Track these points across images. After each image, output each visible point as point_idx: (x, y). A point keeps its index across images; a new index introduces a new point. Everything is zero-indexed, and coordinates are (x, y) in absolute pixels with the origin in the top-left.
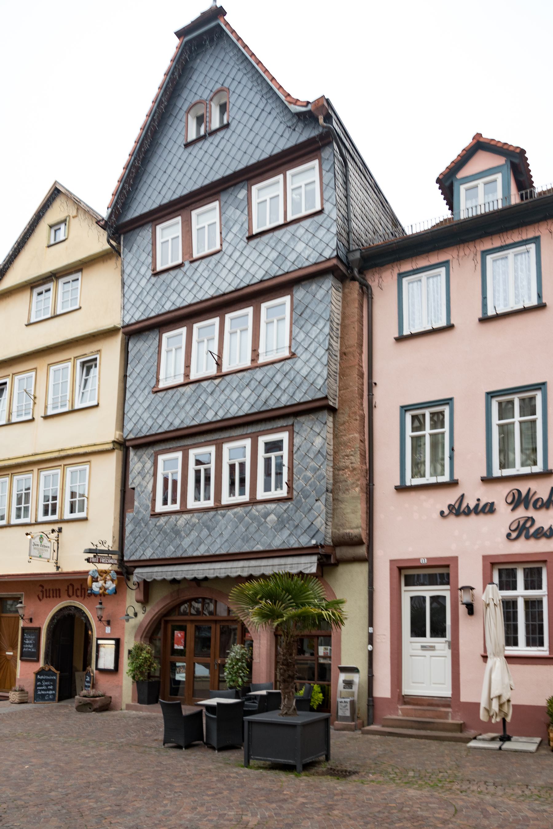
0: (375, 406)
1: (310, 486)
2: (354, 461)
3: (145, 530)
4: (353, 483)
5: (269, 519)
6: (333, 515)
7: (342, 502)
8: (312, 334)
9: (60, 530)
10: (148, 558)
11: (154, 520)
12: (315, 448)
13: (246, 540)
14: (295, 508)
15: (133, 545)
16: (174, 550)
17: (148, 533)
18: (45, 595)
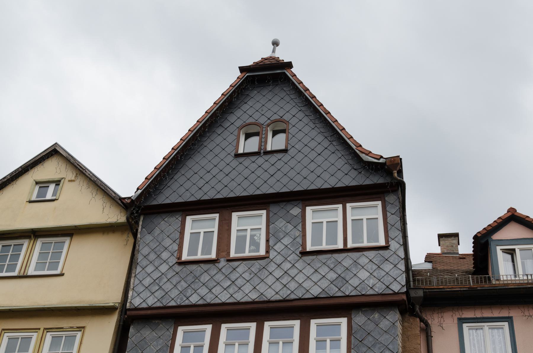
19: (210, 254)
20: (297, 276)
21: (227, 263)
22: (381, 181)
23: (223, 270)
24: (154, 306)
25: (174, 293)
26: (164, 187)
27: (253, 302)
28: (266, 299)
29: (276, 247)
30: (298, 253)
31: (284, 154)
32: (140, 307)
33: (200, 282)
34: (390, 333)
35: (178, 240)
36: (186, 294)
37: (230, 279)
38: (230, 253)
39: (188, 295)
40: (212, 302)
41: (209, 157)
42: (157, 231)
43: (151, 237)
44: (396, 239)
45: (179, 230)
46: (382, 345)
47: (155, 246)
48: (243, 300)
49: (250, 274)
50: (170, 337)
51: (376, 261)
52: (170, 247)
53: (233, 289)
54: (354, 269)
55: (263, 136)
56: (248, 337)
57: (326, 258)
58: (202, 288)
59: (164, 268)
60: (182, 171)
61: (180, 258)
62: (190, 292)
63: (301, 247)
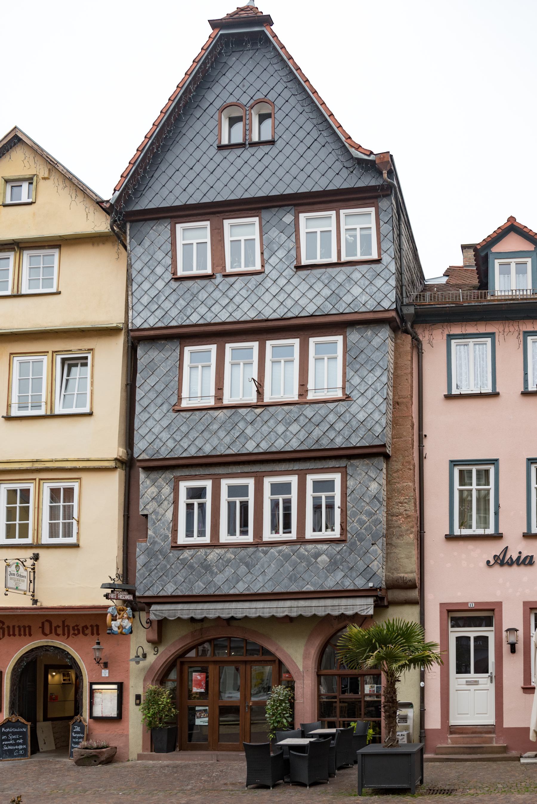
0: (425, 458)
1: (365, 529)
2: (408, 508)
3: (164, 562)
4: (408, 530)
5: (319, 559)
6: (387, 559)
7: (396, 547)
8: (368, 380)
9: (36, 557)
10: (169, 594)
11: (176, 552)
12: (371, 493)
13: (293, 579)
14: (349, 550)
15: (148, 579)
16: (204, 587)
17: (168, 567)
18: (6, 633)
19: (206, 269)
20: (292, 293)
21: (223, 279)
22: (373, 183)
23: (220, 287)
24: (156, 326)
25: (174, 312)
26: (145, 187)
27: (252, 321)
28: (264, 318)
29: (270, 261)
30: (293, 267)
31: (272, 146)
32: (142, 327)
33: (198, 301)
34: (381, 350)
35: (170, 253)
36: (186, 313)
37: (227, 297)
38: (225, 267)
39: (188, 314)
40: (213, 321)
41: (191, 148)
42: (147, 242)
43: (141, 250)
44: (388, 252)
45: (170, 240)
46: (373, 362)
47: (148, 260)
48: (242, 319)
49: (247, 291)
50: (177, 357)
51: (369, 275)
52: (163, 261)
53: (232, 307)
54: (347, 285)
55: (248, 122)
56: (251, 357)
57: (320, 273)
58: (201, 306)
59: (160, 285)
60: (163, 167)
61: (175, 273)
62: (189, 311)
63: (295, 262)
